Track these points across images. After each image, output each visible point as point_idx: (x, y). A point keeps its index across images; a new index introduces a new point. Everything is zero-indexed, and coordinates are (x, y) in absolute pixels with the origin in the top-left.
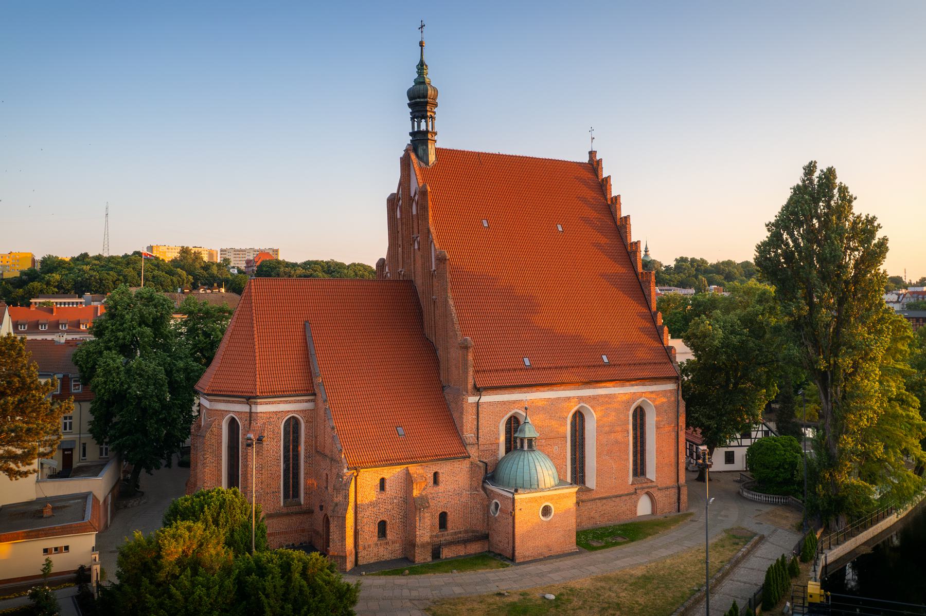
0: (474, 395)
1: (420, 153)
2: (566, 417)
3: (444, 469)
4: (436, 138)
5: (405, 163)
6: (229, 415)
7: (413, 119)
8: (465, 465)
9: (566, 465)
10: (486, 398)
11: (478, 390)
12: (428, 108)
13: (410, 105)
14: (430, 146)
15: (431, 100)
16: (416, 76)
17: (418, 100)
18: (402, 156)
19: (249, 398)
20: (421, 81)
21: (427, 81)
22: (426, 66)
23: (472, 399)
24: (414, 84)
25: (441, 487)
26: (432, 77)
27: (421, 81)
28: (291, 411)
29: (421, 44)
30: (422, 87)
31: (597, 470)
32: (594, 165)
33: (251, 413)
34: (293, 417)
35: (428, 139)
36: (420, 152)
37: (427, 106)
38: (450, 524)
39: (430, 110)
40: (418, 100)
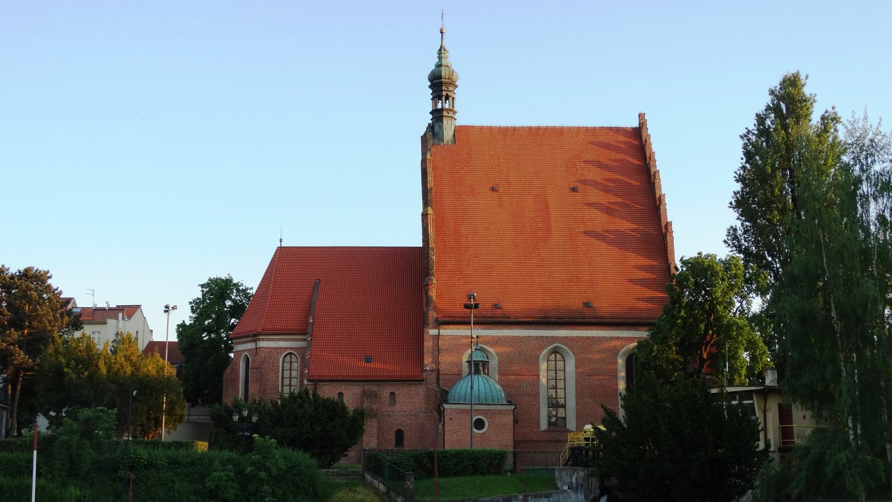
0: (435, 328)
1: (436, 129)
2: (539, 356)
3: (401, 391)
4: (456, 116)
5: (424, 139)
6: (244, 354)
8: (421, 390)
9: (539, 403)
10: (448, 332)
11: (441, 323)
12: (444, 88)
13: (430, 87)
15: (447, 80)
16: (437, 60)
17: (435, 81)
18: (422, 135)
19: (254, 335)
21: (444, 62)
22: (445, 50)
23: (433, 332)
24: (435, 68)
25: (398, 407)
28: (289, 348)
29: (442, 32)
30: (437, 69)
31: (577, 411)
33: (257, 348)
34: (291, 354)
35: (443, 116)
36: (436, 128)
37: (442, 86)
38: (405, 442)
39: (446, 89)
40: (435, 81)
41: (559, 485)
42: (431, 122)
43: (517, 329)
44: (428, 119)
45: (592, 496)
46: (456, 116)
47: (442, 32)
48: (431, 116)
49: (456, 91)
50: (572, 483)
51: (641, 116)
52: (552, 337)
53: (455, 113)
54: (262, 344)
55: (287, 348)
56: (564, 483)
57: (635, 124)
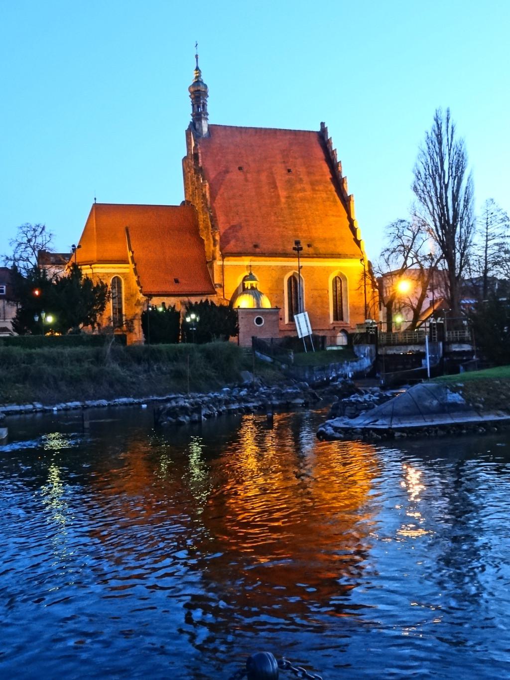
7: (193, 105)
14: (203, 121)
20: (198, 82)
26: (205, 78)
27: (198, 82)
32: (324, 130)
36: (197, 126)
41: (358, 355)
42: (192, 121)
43: (270, 261)
44: (190, 119)
45: (373, 360)
46: (208, 117)
47: (197, 56)
48: (192, 118)
49: (207, 99)
50: (365, 353)
51: (322, 124)
52: (291, 267)
53: (207, 114)
54: (95, 271)
55: (114, 273)
56: (362, 354)
57: (318, 129)
